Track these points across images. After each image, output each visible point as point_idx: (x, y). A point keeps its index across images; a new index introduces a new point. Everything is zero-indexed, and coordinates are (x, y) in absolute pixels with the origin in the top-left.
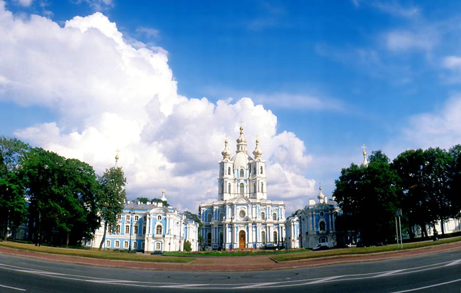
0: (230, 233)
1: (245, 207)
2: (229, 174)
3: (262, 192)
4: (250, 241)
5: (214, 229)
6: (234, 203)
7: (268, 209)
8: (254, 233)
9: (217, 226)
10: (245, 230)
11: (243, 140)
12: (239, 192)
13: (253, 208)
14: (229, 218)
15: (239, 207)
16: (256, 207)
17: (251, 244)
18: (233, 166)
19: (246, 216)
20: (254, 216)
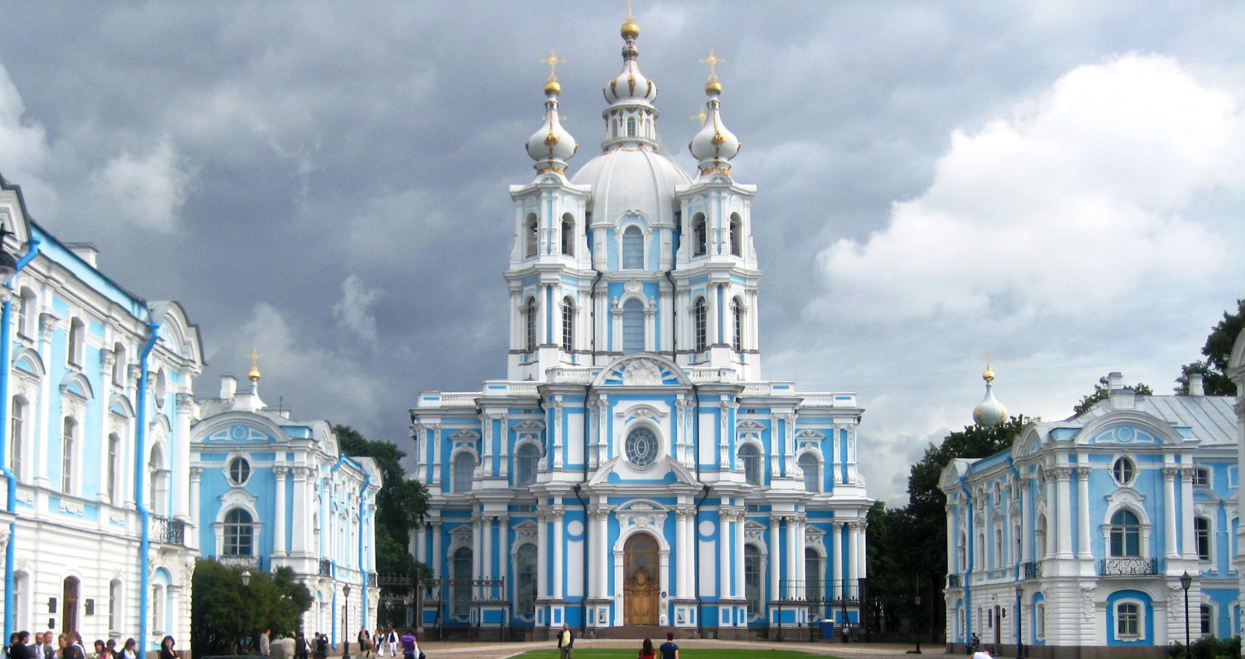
0: (575, 549)
1: (661, 406)
2: (567, 249)
3: (738, 349)
4: (686, 590)
5: (487, 531)
6: (598, 382)
7: (775, 426)
8: (707, 549)
9: (500, 510)
10: (658, 531)
11: (641, 81)
12: (618, 346)
13: (701, 416)
14: (567, 468)
15: (623, 406)
16: (717, 411)
17: (687, 609)
18: (588, 215)
20: (707, 458)
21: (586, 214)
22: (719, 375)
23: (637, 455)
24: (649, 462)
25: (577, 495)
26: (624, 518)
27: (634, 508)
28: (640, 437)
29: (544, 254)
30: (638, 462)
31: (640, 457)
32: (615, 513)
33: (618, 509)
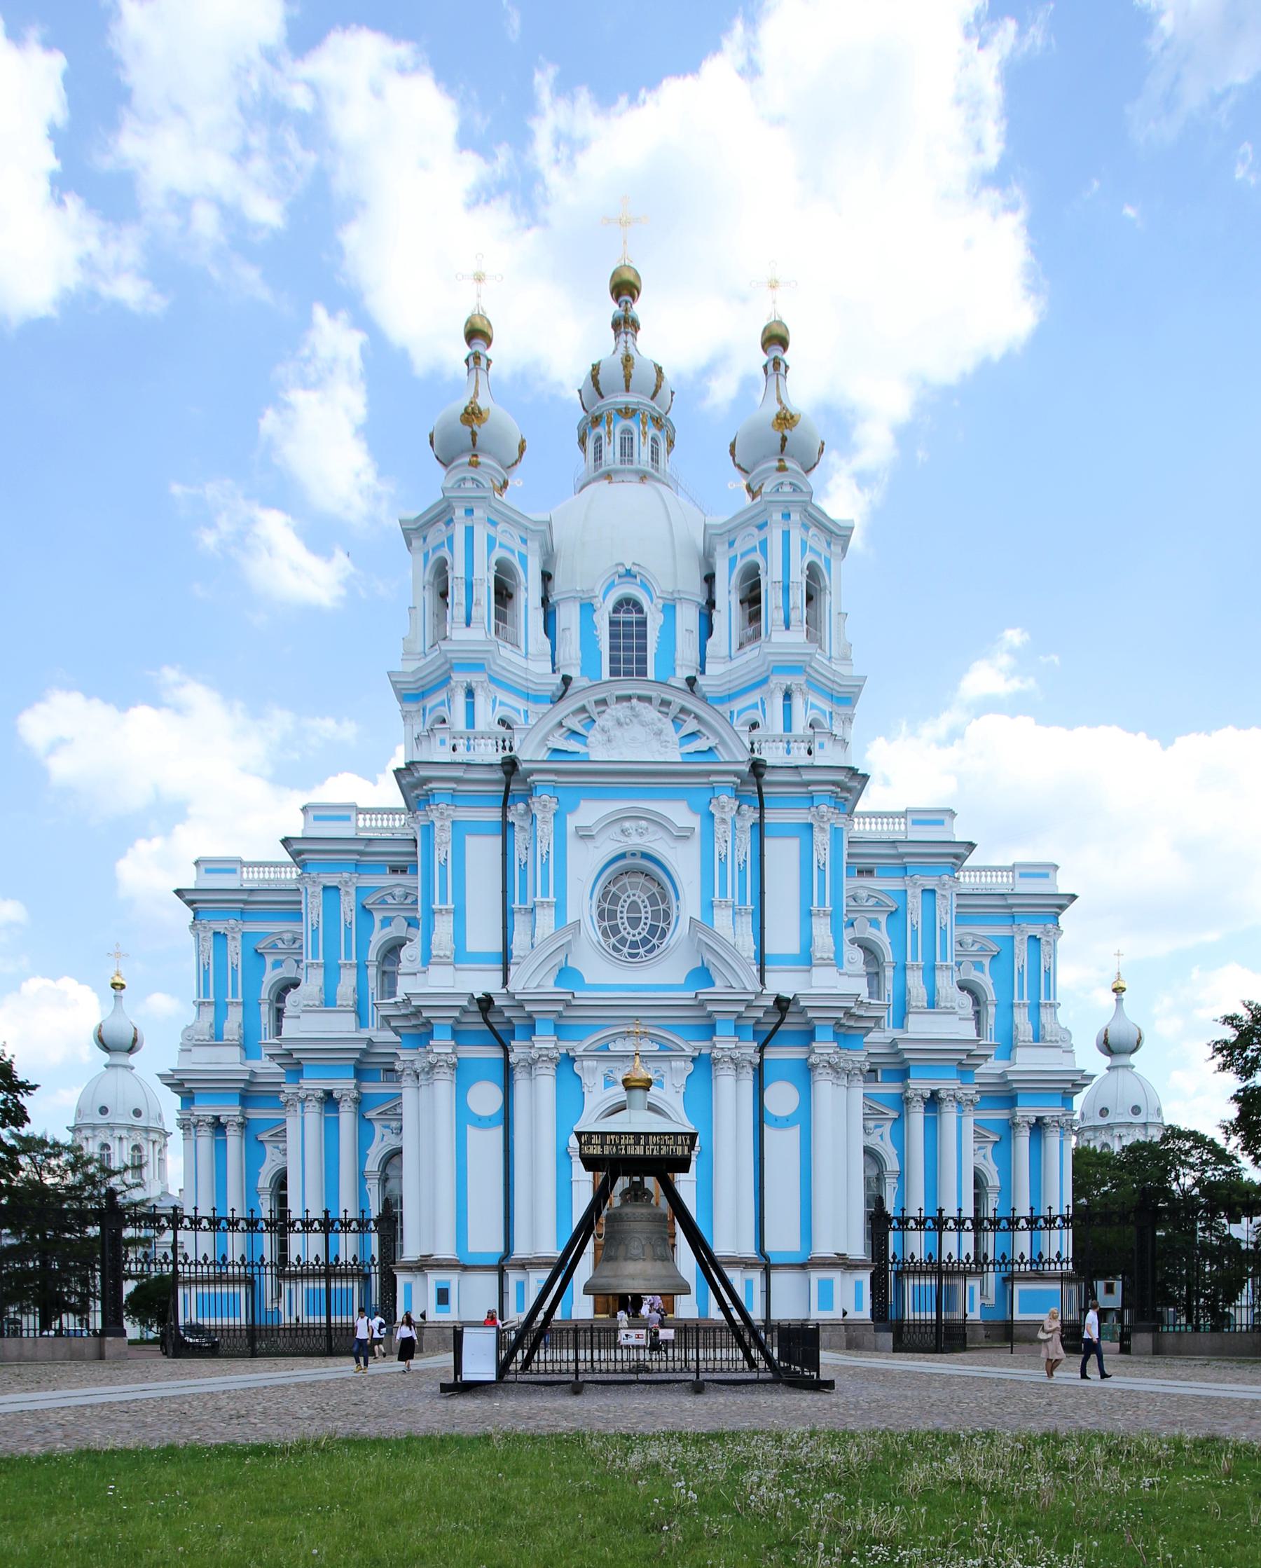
0: (485, 1145)
13: (767, 842)
14: (461, 957)
18: (547, 577)
19: (679, 932)
21: (543, 580)
22: (810, 752)
23: (624, 933)
24: (654, 947)
25: (487, 1022)
26: (594, 1070)
27: (618, 1047)
28: (630, 892)
29: (459, 625)
30: (626, 950)
31: (630, 938)
32: (573, 1060)
33: (579, 1051)
